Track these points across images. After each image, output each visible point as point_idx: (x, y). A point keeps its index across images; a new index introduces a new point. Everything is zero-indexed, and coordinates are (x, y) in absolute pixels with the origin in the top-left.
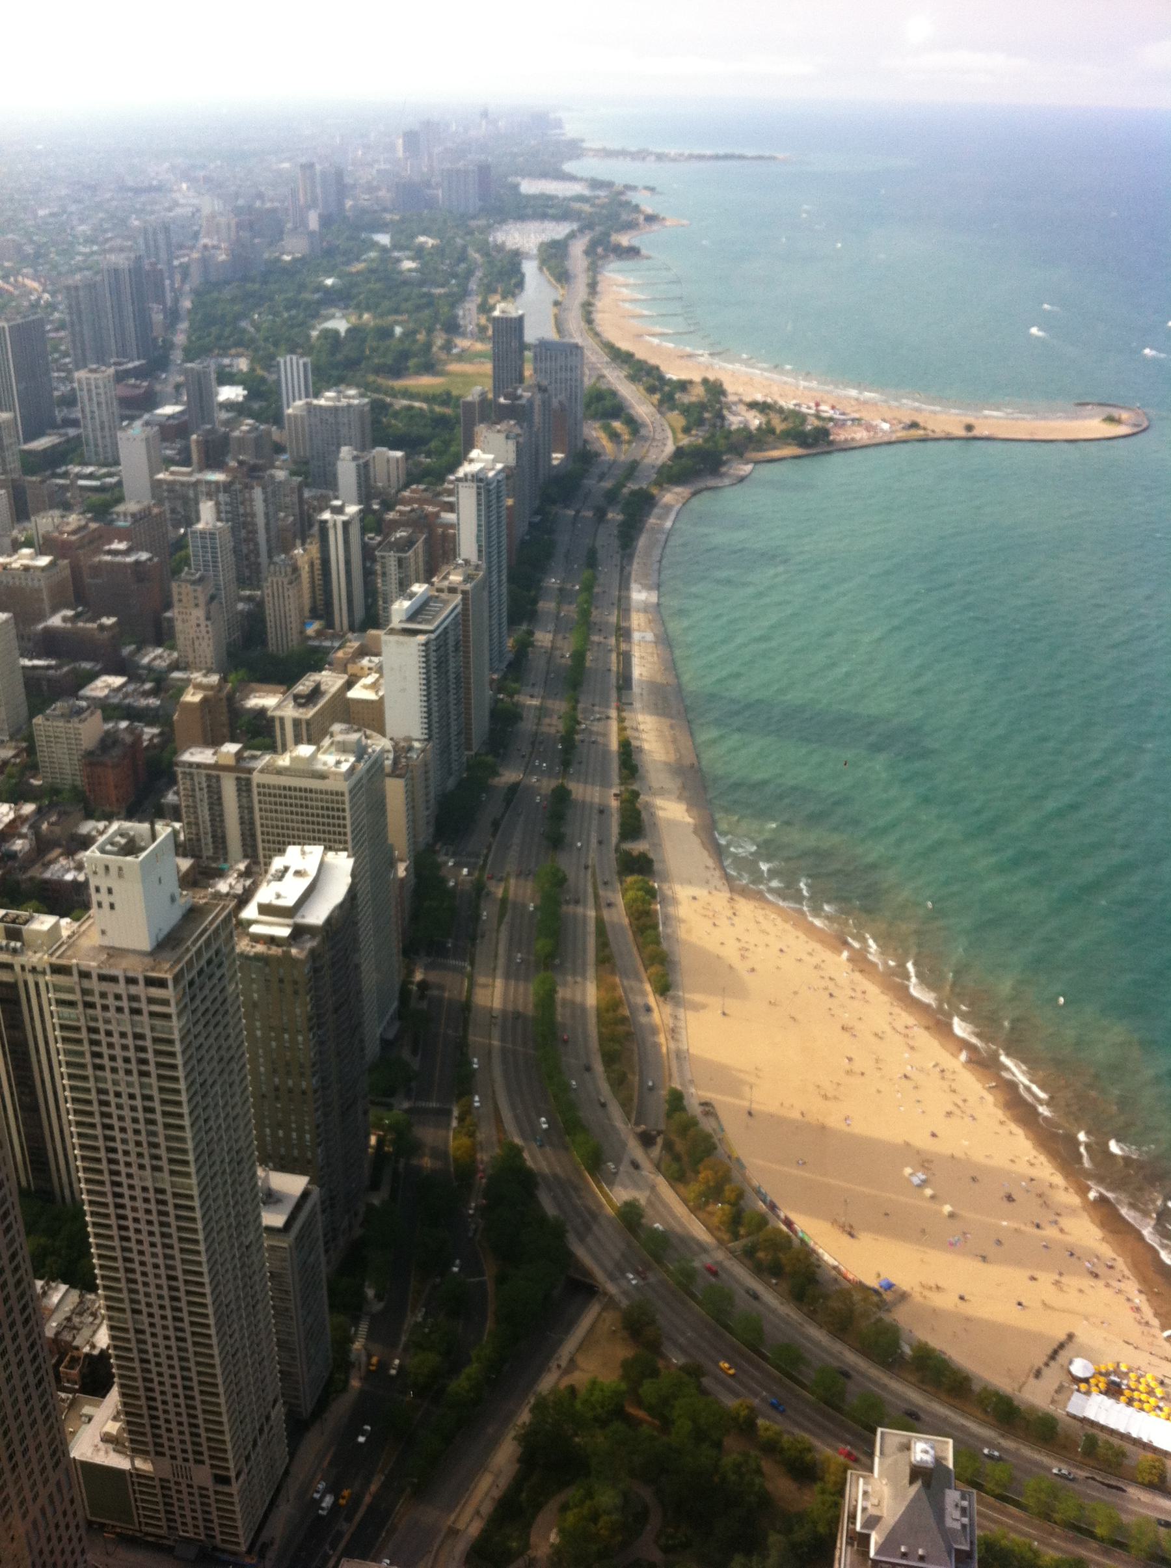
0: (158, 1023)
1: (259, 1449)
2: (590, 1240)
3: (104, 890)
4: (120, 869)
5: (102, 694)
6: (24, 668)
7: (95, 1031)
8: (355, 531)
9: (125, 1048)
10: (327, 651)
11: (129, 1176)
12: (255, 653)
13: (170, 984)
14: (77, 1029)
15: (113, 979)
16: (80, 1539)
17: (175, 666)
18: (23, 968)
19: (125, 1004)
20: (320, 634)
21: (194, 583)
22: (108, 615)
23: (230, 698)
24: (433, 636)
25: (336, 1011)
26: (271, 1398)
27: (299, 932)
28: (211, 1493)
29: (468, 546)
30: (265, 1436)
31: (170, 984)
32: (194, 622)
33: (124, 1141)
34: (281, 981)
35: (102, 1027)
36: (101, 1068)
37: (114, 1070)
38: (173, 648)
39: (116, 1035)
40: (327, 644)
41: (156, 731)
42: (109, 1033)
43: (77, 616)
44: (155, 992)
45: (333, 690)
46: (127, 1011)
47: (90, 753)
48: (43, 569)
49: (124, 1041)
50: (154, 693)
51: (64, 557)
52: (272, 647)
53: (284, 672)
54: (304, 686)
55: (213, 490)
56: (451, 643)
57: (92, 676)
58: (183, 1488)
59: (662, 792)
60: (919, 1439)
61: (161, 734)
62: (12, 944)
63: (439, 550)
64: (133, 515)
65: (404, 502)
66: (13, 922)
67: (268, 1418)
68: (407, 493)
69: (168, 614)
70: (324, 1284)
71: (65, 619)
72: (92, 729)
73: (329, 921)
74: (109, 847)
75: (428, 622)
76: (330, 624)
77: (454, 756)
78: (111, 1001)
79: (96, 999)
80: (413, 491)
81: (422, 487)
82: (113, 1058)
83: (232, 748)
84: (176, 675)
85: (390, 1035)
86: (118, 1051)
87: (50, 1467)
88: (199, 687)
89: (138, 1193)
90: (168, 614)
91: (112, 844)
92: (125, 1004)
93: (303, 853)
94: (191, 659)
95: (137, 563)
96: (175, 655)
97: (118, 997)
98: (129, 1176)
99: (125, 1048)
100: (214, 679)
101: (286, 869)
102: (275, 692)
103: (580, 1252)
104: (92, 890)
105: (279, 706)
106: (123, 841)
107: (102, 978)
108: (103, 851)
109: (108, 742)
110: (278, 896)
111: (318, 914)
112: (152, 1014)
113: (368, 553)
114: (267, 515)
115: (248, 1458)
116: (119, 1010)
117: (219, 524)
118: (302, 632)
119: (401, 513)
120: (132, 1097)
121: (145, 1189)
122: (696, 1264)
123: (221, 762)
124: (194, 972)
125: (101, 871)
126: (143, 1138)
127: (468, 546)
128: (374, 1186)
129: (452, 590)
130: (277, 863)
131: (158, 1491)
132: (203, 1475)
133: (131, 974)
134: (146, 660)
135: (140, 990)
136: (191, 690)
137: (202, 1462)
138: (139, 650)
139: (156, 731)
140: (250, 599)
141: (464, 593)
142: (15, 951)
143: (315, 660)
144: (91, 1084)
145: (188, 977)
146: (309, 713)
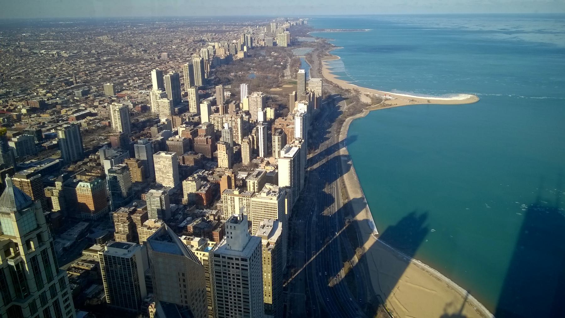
0: (244, 272)
3: (229, 233)
7: (225, 273)
14: (220, 273)
15: (232, 259)
19: (235, 266)
35: (228, 273)
97: (233, 264)
107: (229, 258)
127: (298, 133)
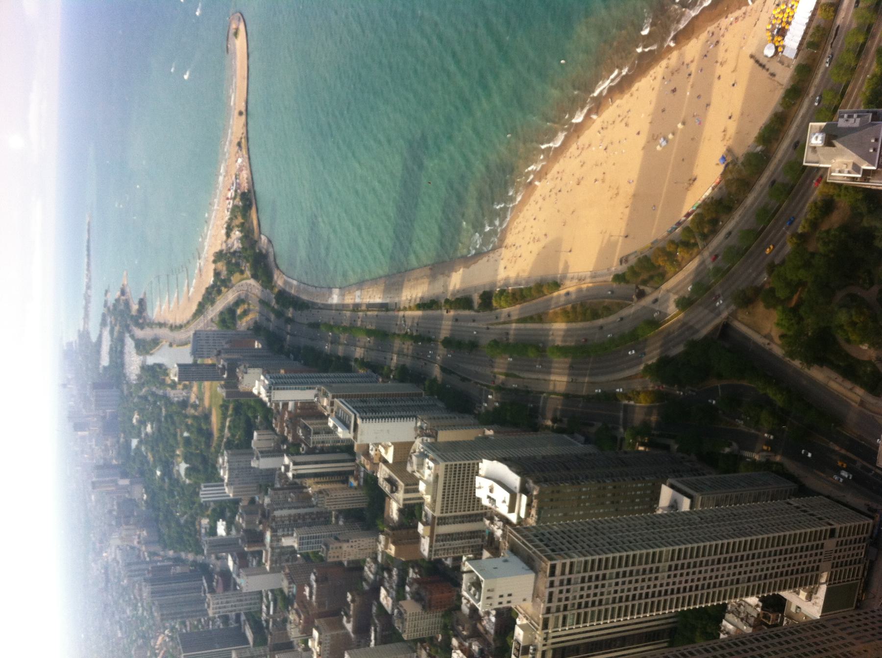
0: (575, 569)
1: (815, 513)
2: (697, 327)
3: (501, 600)
4: (489, 590)
5: (390, 601)
6: (376, 644)
8: (299, 459)
9: (589, 588)
10: (366, 474)
11: (661, 585)
12: (368, 514)
13: (553, 562)
14: (579, 615)
15: (551, 594)
16: (866, 613)
17: (375, 560)
18: (544, 645)
19: (565, 588)
20: (357, 478)
21: (328, 549)
22: (346, 597)
23: (393, 529)
24: (358, 415)
25: (568, 469)
26: (787, 506)
27: (524, 490)
28: (840, 539)
29: (307, 395)
30: (808, 509)
31: (553, 562)
32: (350, 549)
33: (642, 588)
34: (552, 500)
36: (601, 601)
37: (602, 594)
38: (364, 561)
39: (582, 593)
40: (362, 474)
41: (411, 571)
42: (581, 597)
43: (347, 615)
44: (558, 571)
45: (388, 471)
46: (568, 587)
47: (424, 608)
48: (320, 634)
49: (586, 589)
50: (390, 571)
51: (313, 622)
52: (364, 505)
53: (378, 499)
54: (386, 487)
55: (276, 538)
56: (361, 404)
57: (381, 606)
58: (837, 555)
59: (446, 286)
60: (810, 141)
61: (413, 568)
62: (531, 651)
63: (310, 411)
64: (290, 583)
65: (282, 431)
66: (518, 650)
67: (798, 508)
68: (278, 430)
69: (346, 563)
70: (723, 476)
71: (348, 622)
72: (410, 607)
73: (518, 473)
74: (477, 597)
75: (350, 418)
76: (351, 473)
77: (425, 403)
78: (563, 596)
79: (562, 604)
80: (276, 426)
81: (274, 421)
82: (595, 595)
83: (421, 528)
84: (380, 559)
85: (582, 439)
86: (591, 592)
87: (825, 630)
88: (386, 546)
89: (671, 581)
90: (346, 563)
91: (475, 595)
92: (565, 588)
93: (480, 488)
94: (371, 551)
95: (316, 581)
96: (368, 559)
97: (561, 592)
98: (661, 585)
99: (589, 588)
100: (382, 538)
101: (489, 497)
102: (389, 504)
103: (704, 332)
104: (501, 606)
105: (397, 502)
106: (473, 589)
107: (550, 601)
108: (479, 600)
109: (417, 597)
110: (504, 502)
111: (515, 480)
112: (571, 572)
113: (311, 451)
114: (289, 508)
115: (820, 519)
116: (568, 591)
117: (295, 535)
118: (356, 488)
119: (289, 432)
120: (617, 584)
121: (669, 577)
122: (711, 267)
123: (429, 534)
124: (547, 549)
125: (490, 601)
126: (640, 578)
127: (307, 395)
128: (667, 448)
129: (332, 404)
130: (485, 502)
131: (839, 569)
132: (830, 544)
133: (548, 585)
134: (372, 576)
135: (557, 580)
136: (388, 551)
137: (823, 544)
138: (365, 580)
139: (411, 571)
140: (337, 518)
141: (333, 397)
142: (535, 650)
143: (371, 481)
144: (610, 607)
145: (550, 552)
146: (401, 484)
